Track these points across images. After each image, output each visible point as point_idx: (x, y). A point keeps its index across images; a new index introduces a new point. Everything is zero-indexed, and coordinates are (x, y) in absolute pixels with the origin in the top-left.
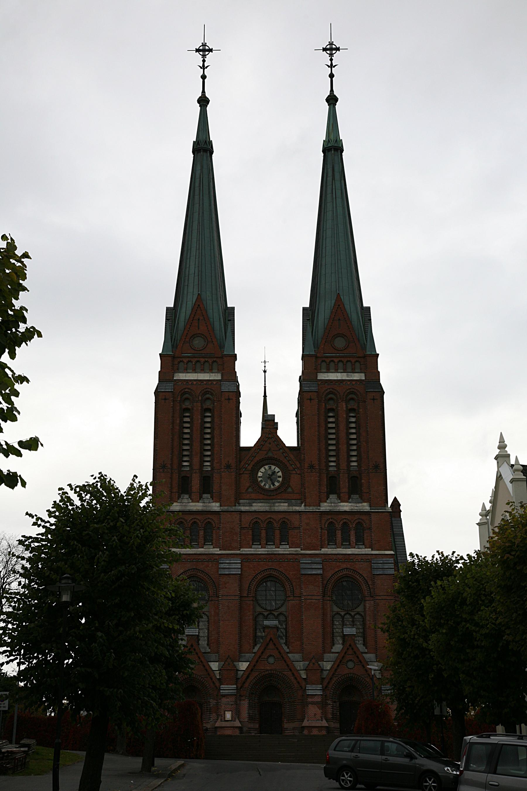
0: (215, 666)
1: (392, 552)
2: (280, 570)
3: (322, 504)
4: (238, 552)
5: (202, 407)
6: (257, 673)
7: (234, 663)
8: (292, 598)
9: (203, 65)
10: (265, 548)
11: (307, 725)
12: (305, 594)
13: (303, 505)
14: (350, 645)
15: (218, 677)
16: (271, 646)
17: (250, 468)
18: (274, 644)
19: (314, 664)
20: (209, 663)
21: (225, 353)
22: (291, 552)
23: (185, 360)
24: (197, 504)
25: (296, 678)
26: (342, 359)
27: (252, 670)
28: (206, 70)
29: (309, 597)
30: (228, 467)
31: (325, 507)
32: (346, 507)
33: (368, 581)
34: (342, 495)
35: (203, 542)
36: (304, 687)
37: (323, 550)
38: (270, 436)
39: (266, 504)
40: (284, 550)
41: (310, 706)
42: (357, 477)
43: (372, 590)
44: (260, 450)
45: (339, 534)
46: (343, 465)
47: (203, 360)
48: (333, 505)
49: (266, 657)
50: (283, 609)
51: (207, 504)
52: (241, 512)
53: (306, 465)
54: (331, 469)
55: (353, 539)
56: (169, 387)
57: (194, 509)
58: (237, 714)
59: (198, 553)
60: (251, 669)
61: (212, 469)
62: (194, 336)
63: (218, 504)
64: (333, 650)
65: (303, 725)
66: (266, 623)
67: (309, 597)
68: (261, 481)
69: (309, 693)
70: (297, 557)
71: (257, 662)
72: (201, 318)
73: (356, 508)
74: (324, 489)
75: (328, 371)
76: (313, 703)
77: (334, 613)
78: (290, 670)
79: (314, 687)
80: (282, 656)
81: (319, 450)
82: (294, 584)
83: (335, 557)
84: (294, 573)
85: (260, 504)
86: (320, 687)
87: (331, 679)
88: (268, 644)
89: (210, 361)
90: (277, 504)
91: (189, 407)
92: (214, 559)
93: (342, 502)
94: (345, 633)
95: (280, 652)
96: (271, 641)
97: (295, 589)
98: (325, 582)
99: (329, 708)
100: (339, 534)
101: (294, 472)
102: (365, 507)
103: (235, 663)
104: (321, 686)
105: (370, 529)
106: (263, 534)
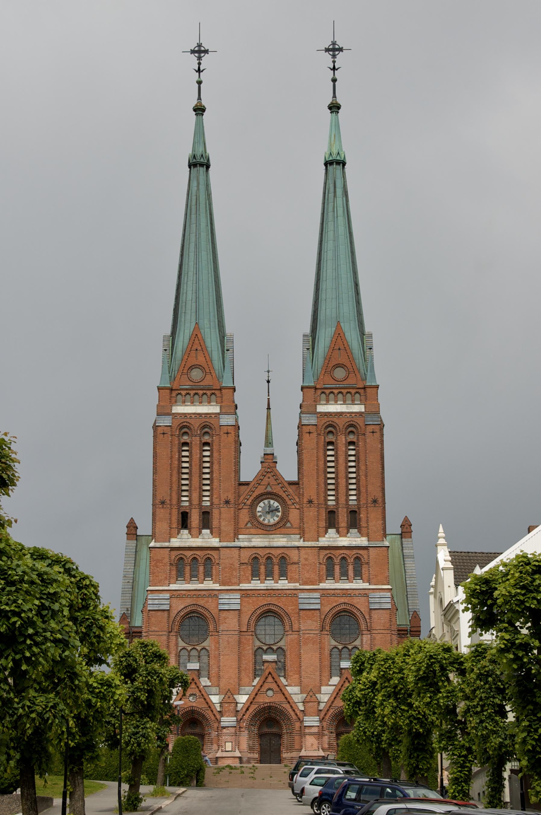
0: (215, 699)
1: (389, 587)
2: (279, 605)
3: (320, 539)
4: (238, 588)
5: (201, 441)
6: (257, 706)
7: (234, 696)
8: (290, 632)
9: (199, 68)
10: (264, 583)
11: (305, 755)
12: (302, 628)
13: (302, 540)
14: (347, 679)
15: (219, 710)
16: (270, 679)
17: (249, 502)
18: (273, 678)
19: (311, 696)
20: (210, 696)
21: (224, 385)
22: (290, 588)
23: (184, 393)
24: (197, 540)
25: (294, 710)
26: (342, 390)
27: (251, 703)
28: (201, 73)
29: (307, 632)
30: (227, 502)
31: (324, 541)
32: (344, 541)
33: (365, 615)
34: (340, 530)
35: (203, 578)
36: (301, 719)
37: (321, 584)
38: (269, 470)
39: (265, 540)
40: (283, 584)
41: (307, 737)
42: (356, 512)
43: (369, 624)
44: (259, 484)
45: (337, 568)
46: (342, 500)
47: (201, 392)
48: (331, 540)
49: (265, 690)
50: (281, 644)
51: (206, 540)
52: (240, 547)
53: (305, 500)
54: (330, 503)
55: (351, 573)
56: (166, 421)
57: (194, 545)
58: (238, 744)
59: (198, 588)
60: (251, 702)
61: (212, 504)
62: (192, 368)
63: (217, 540)
64: (330, 683)
65: (301, 755)
66: (266, 657)
67: (307, 632)
68: (260, 516)
69: (306, 724)
70: (295, 592)
71: (256, 694)
72: (199, 348)
73: (354, 543)
74: (323, 524)
75: (328, 402)
76: (311, 734)
77: (332, 647)
78: (289, 702)
79: (312, 718)
80: (281, 690)
81: (318, 484)
82: (293, 619)
83: (333, 592)
84: (292, 608)
85: (259, 540)
86: (317, 718)
87: (328, 710)
88: (267, 678)
89: (209, 393)
90: (276, 540)
91: (188, 441)
92: (213, 594)
93: (340, 536)
94: (341, 667)
95: (278, 686)
96: (270, 675)
97: (293, 623)
98: (323, 617)
99: (326, 739)
100: (337, 568)
101: (293, 507)
102: (363, 541)
103: (235, 696)
104: (318, 717)
105: (368, 563)
106: (262, 569)
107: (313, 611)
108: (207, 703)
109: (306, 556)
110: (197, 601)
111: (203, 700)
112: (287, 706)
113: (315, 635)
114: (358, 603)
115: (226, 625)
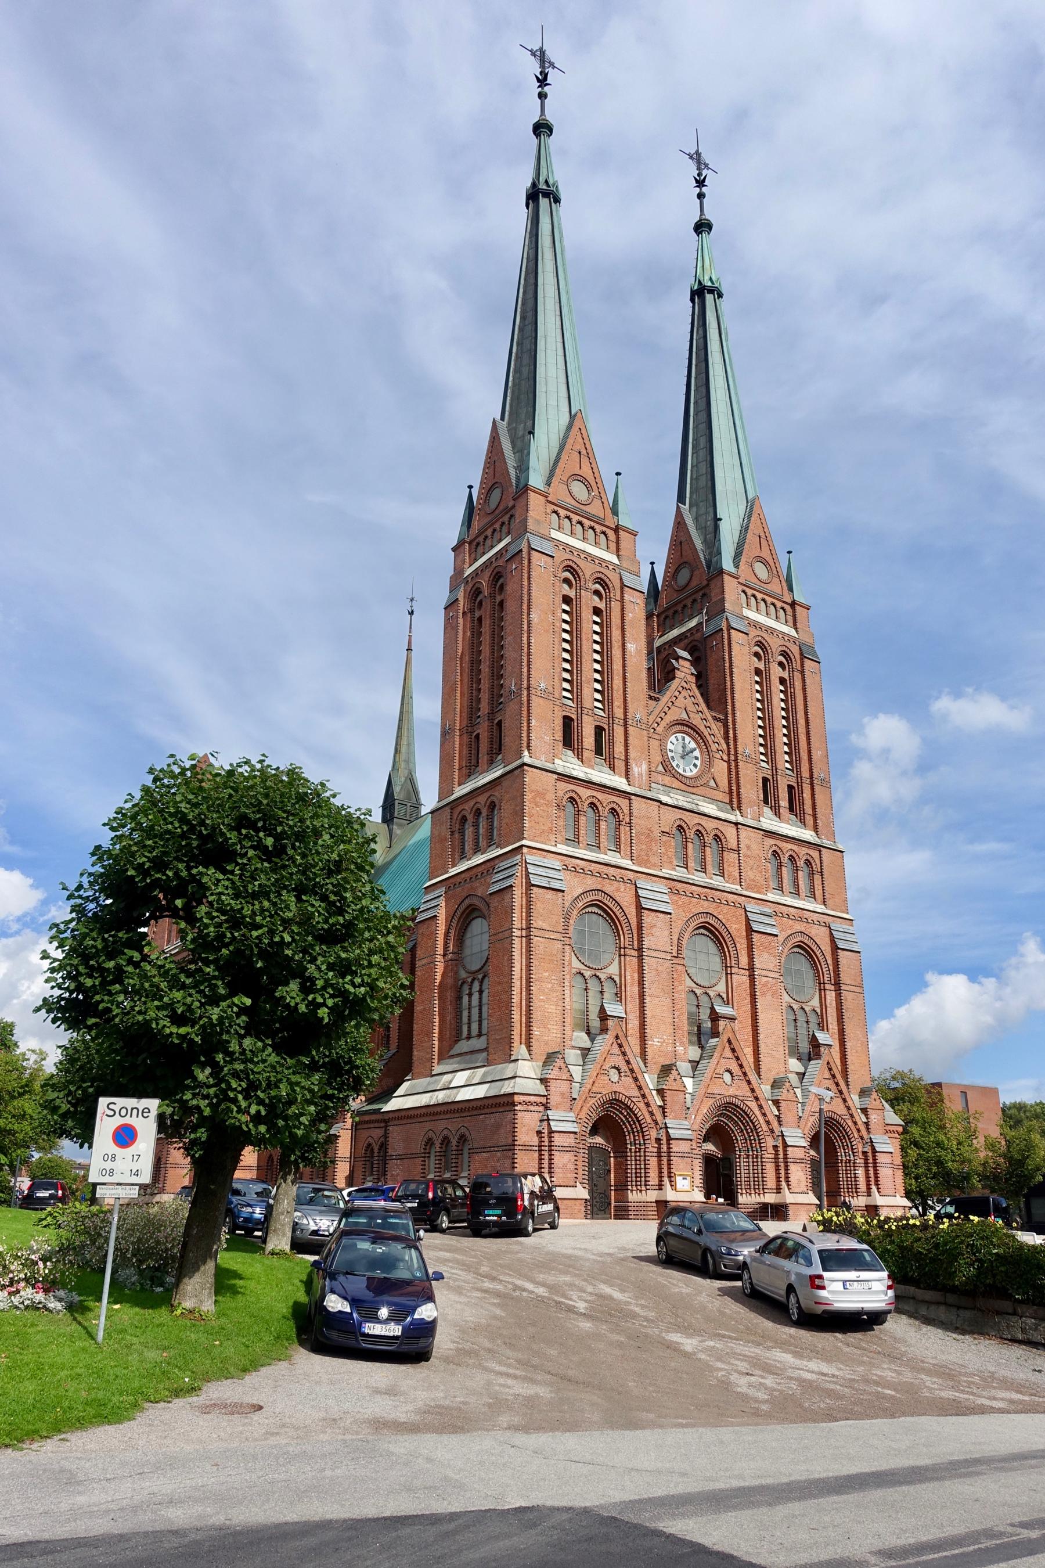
25: (764, 1115)
79: (792, 1130)
107: (770, 937)
108: (640, 1088)
109: (748, 842)
110: (603, 885)
111: (631, 1080)
112: (753, 1105)
113: (774, 981)
114: (817, 935)
115: (652, 939)
